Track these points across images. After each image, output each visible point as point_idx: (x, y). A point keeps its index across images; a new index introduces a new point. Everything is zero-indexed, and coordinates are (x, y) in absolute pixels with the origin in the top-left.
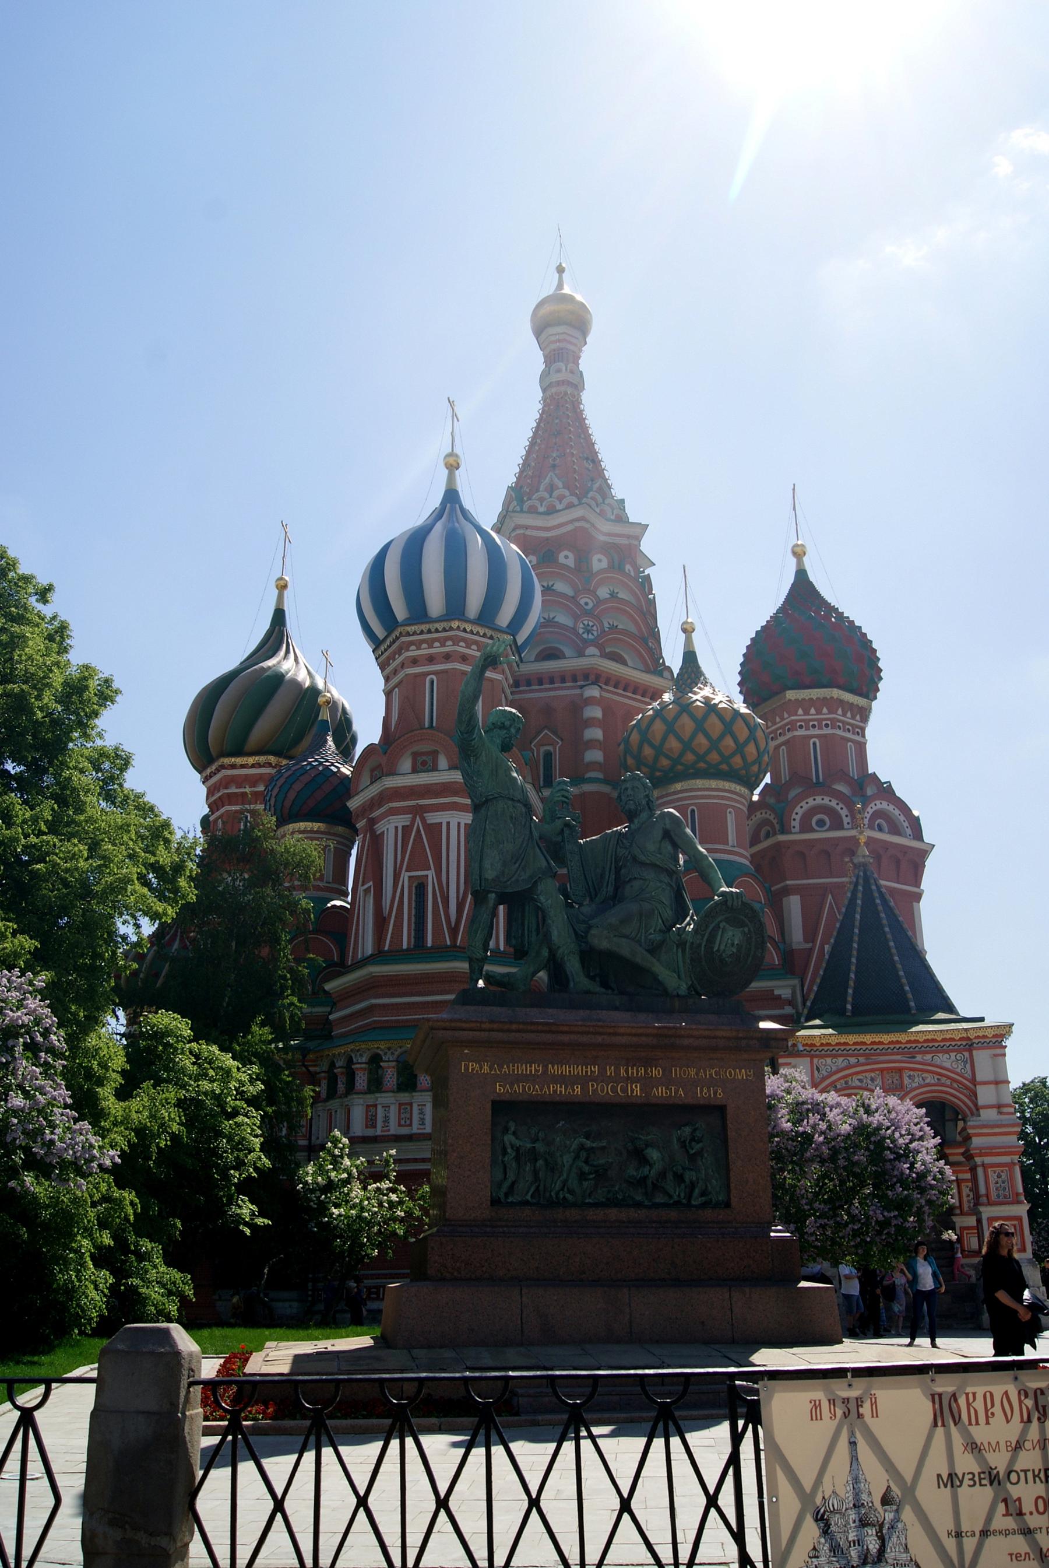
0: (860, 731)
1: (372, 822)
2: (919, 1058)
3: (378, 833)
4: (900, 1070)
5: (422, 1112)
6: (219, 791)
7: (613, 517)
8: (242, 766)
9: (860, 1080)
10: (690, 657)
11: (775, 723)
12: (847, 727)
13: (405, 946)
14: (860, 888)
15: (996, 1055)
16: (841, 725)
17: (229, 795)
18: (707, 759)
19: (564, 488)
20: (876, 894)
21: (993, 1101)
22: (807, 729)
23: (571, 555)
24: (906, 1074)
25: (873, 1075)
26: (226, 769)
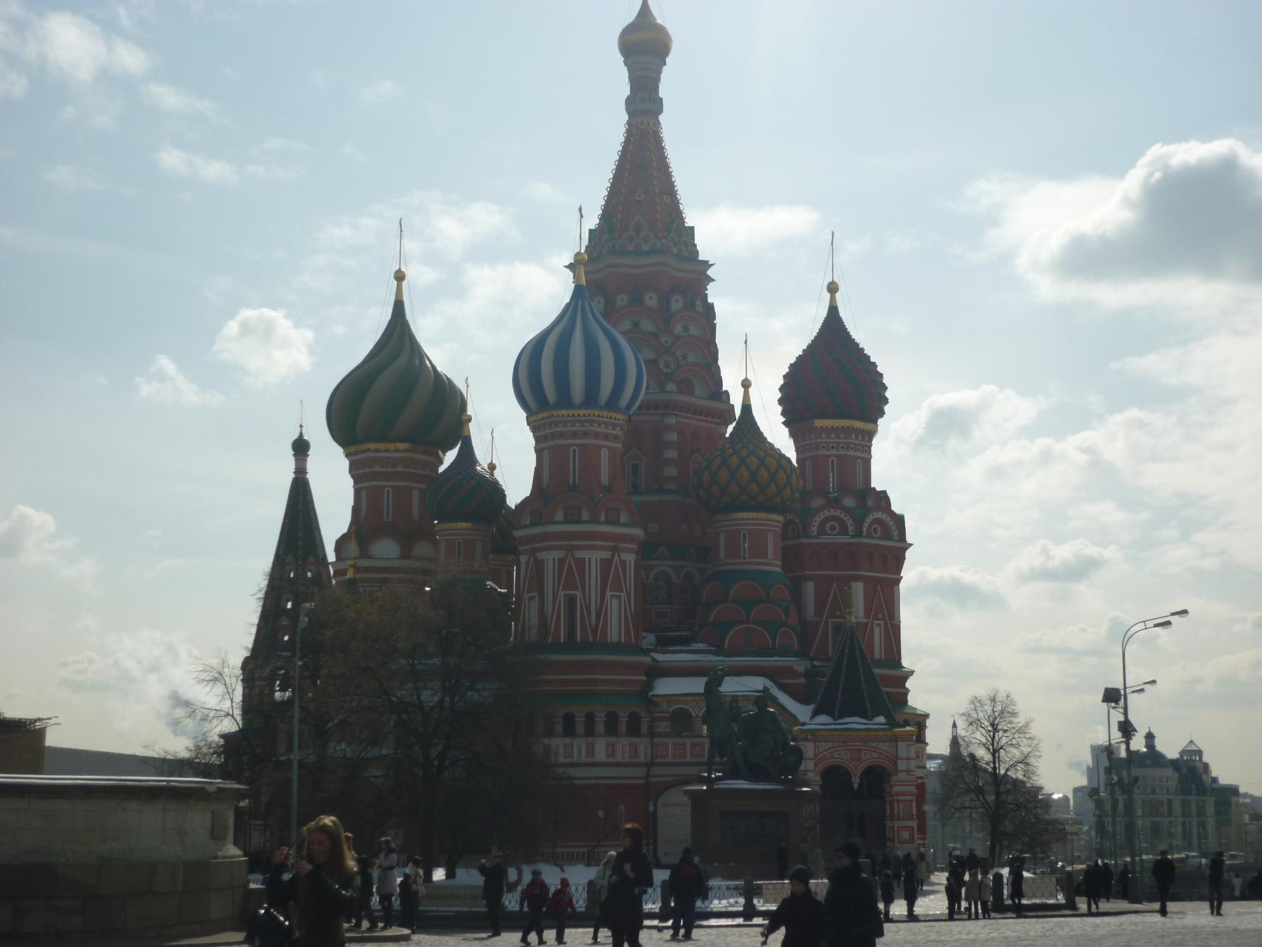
1: (533, 552)
2: (870, 744)
4: (860, 750)
5: (579, 750)
7: (686, 255)
8: (386, 451)
10: (747, 408)
12: (858, 447)
13: (562, 640)
14: (848, 642)
16: (853, 446)
20: (857, 647)
21: (905, 768)
22: (828, 450)
23: (654, 296)
26: (372, 452)
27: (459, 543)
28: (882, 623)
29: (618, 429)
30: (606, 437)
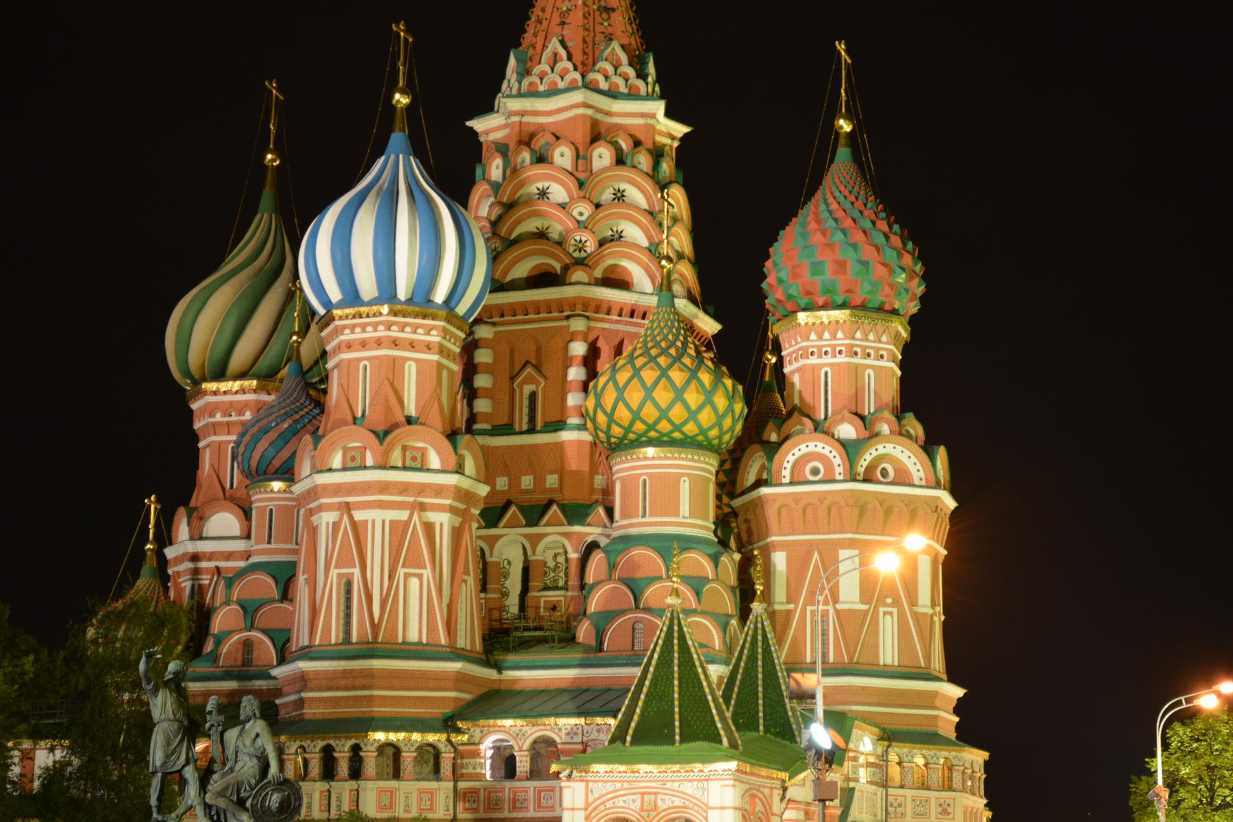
0: (885, 353)
1: (311, 512)
2: (669, 785)
3: (315, 524)
4: (656, 794)
6: (204, 418)
7: (626, 91)
8: (225, 393)
9: (625, 802)
11: (791, 346)
15: (726, 786)
17: (214, 425)
18: (659, 427)
19: (570, 58)
20: (676, 635)
24: (660, 797)
25: (634, 797)
27: (271, 510)
28: (895, 610)
29: (434, 332)
30: (412, 345)
